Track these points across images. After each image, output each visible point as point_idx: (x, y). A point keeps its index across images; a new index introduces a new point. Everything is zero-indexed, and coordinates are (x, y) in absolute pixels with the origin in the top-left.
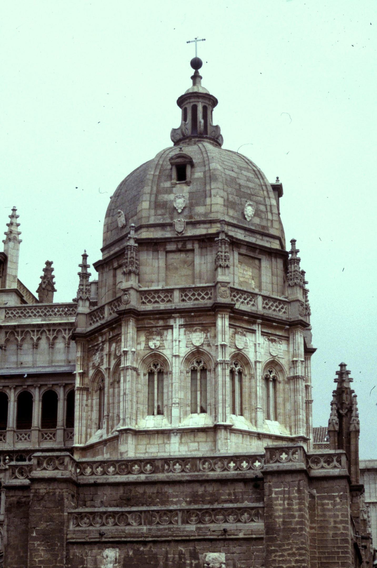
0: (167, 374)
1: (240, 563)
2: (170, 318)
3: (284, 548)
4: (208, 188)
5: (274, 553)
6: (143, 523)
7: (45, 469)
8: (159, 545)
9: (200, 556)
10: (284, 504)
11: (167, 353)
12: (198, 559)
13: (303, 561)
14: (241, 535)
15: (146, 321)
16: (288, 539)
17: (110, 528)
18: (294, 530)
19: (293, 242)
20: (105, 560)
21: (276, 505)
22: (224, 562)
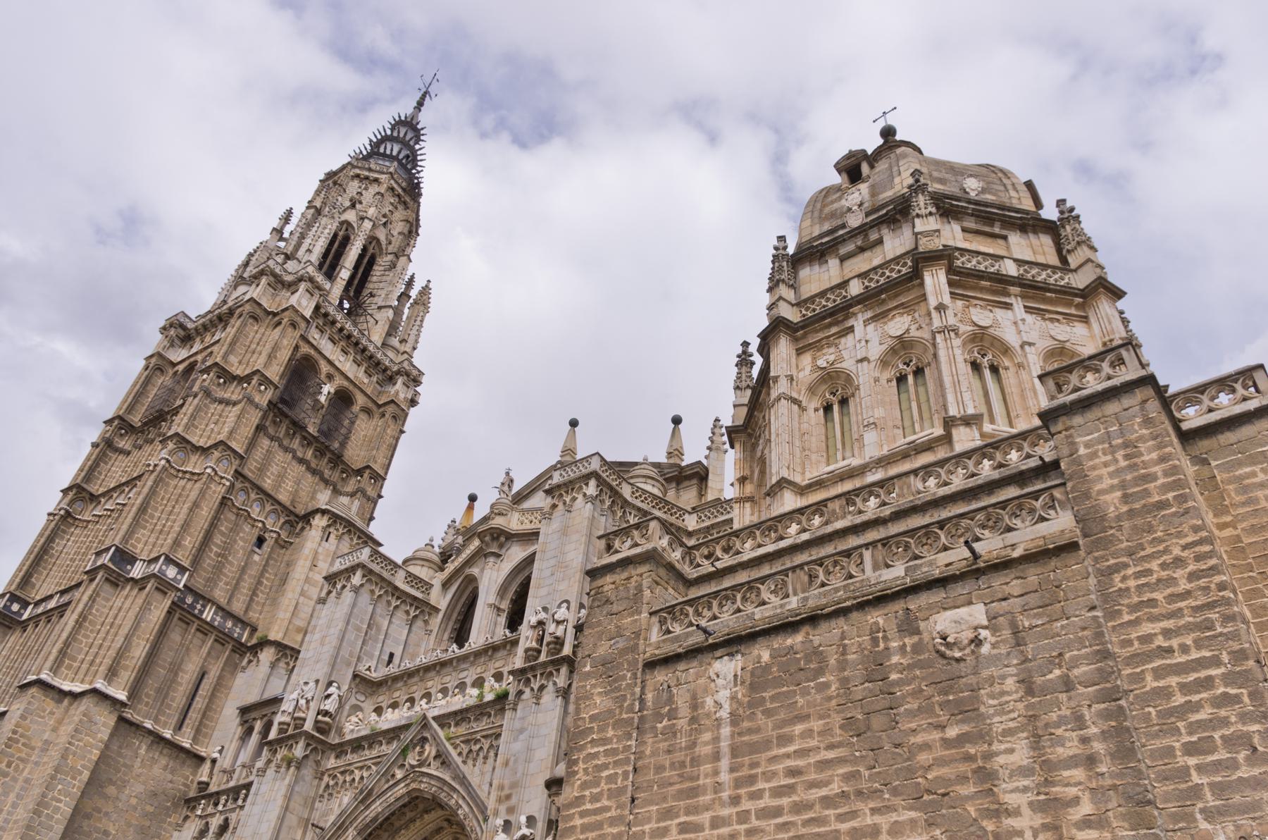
0: (853, 395)
1: (1027, 618)
2: (847, 318)
3: (1142, 553)
4: (895, 169)
5: (1118, 571)
6: (791, 591)
7: (617, 552)
8: (824, 626)
9: (922, 625)
10: (1116, 461)
11: (848, 365)
12: (917, 632)
13: (1214, 570)
14: (1016, 554)
15: (810, 336)
16: (1151, 529)
17: (726, 620)
18: (1162, 505)
19: (1060, 203)
20: (713, 685)
21: (1094, 468)
22: (985, 623)
